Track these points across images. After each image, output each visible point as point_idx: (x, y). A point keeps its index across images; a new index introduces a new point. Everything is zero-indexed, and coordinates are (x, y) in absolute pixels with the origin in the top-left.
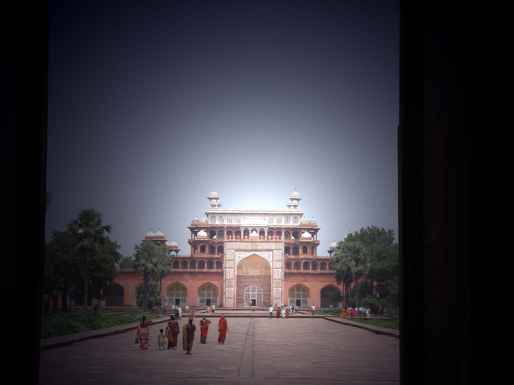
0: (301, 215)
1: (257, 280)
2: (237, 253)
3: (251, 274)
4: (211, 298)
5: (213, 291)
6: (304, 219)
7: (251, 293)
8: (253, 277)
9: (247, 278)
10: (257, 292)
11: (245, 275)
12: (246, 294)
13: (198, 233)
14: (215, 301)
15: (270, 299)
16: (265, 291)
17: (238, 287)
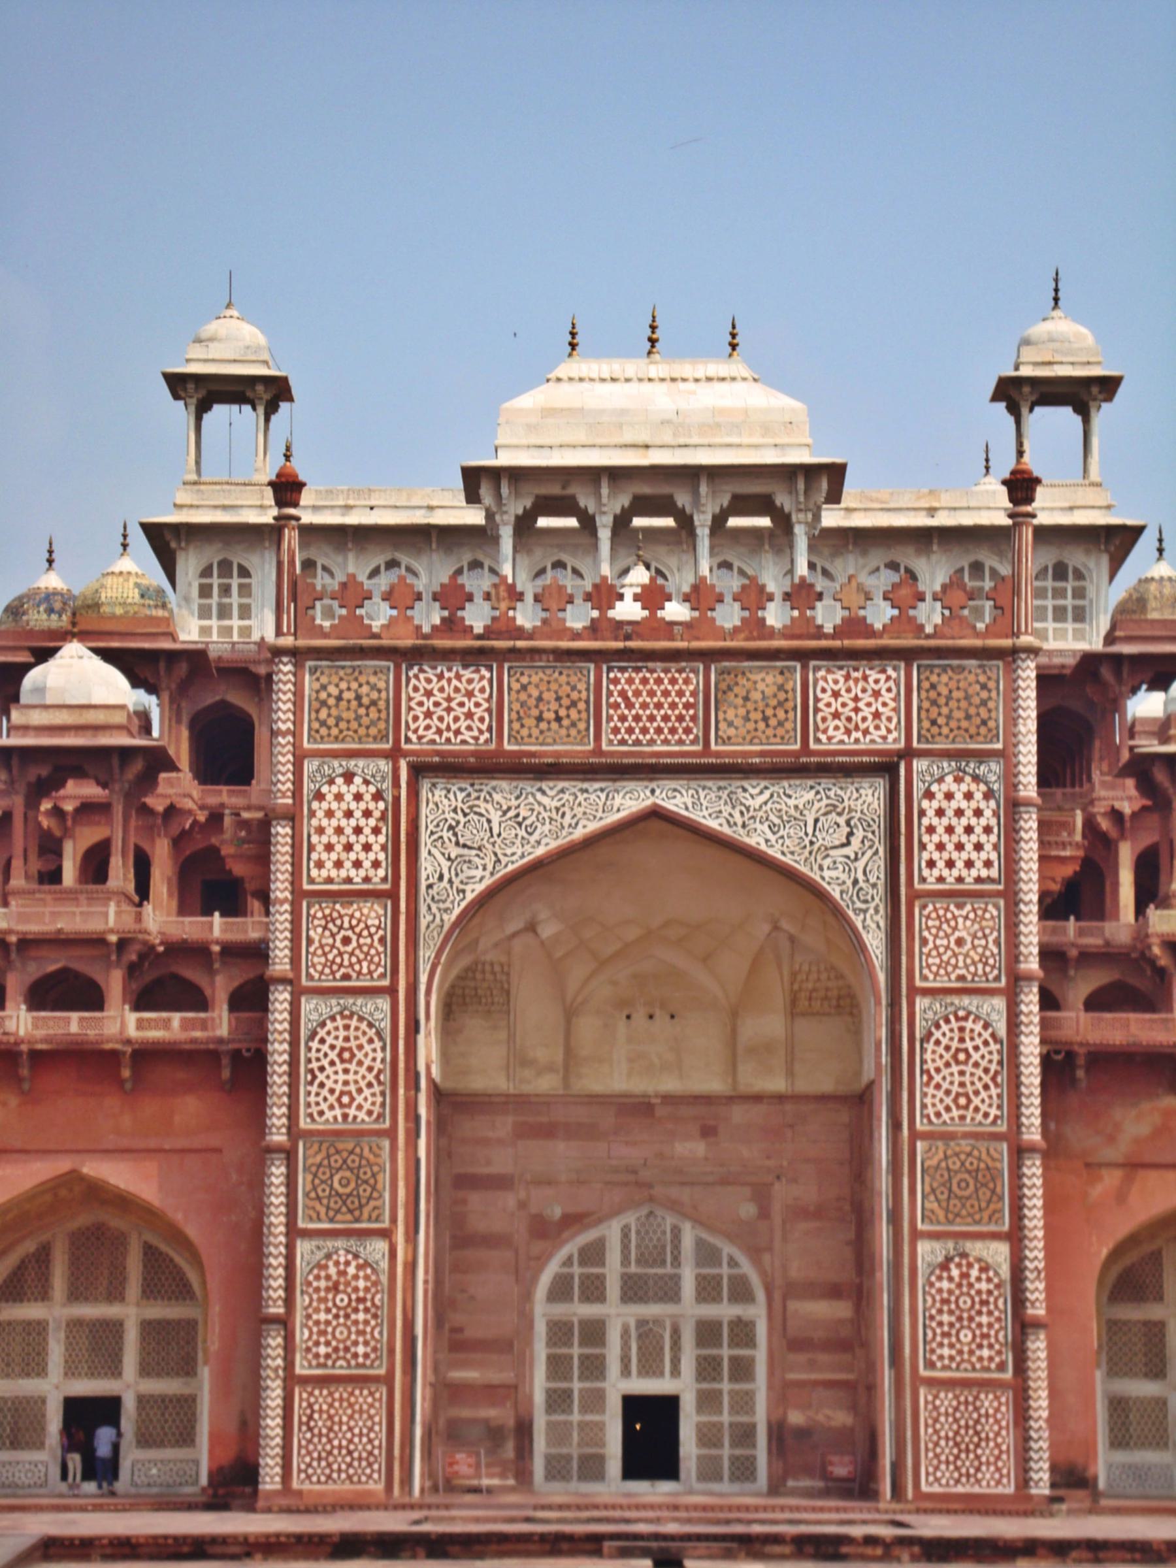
0: (1117, 541)
1: (690, 1149)
2: (440, 801)
3: (617, 1079)
4: (129, 1385)
5: (150, 1291)
6: (1162, 570)
7: (618, 1315)
8: (638, 1109)
9: (573, 1131)
10: (689, 1308)
11: (546, 1084)
12: (559, 1332)
13: (32, 678)
14: (171, 1422)
15: (859, 1395)
16: (793, 1290)
17: (459, 1242)
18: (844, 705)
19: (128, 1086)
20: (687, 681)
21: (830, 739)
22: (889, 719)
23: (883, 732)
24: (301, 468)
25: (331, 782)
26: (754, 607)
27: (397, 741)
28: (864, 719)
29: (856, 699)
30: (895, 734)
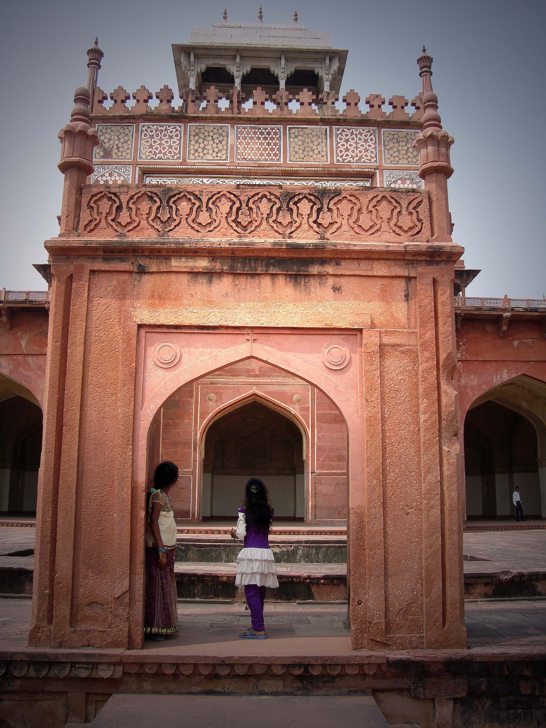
18: (351, 145)
19: (8, 327)
20: (275, 134)
21: (344, 160)
22: (372, 152)
23: (369, 158)
24: (101, 47)
25: (103, 175)
26: (306, 104)
27: (135, 157)
28: (360, 152)
29: (356, 143)
30: (375, 159)
